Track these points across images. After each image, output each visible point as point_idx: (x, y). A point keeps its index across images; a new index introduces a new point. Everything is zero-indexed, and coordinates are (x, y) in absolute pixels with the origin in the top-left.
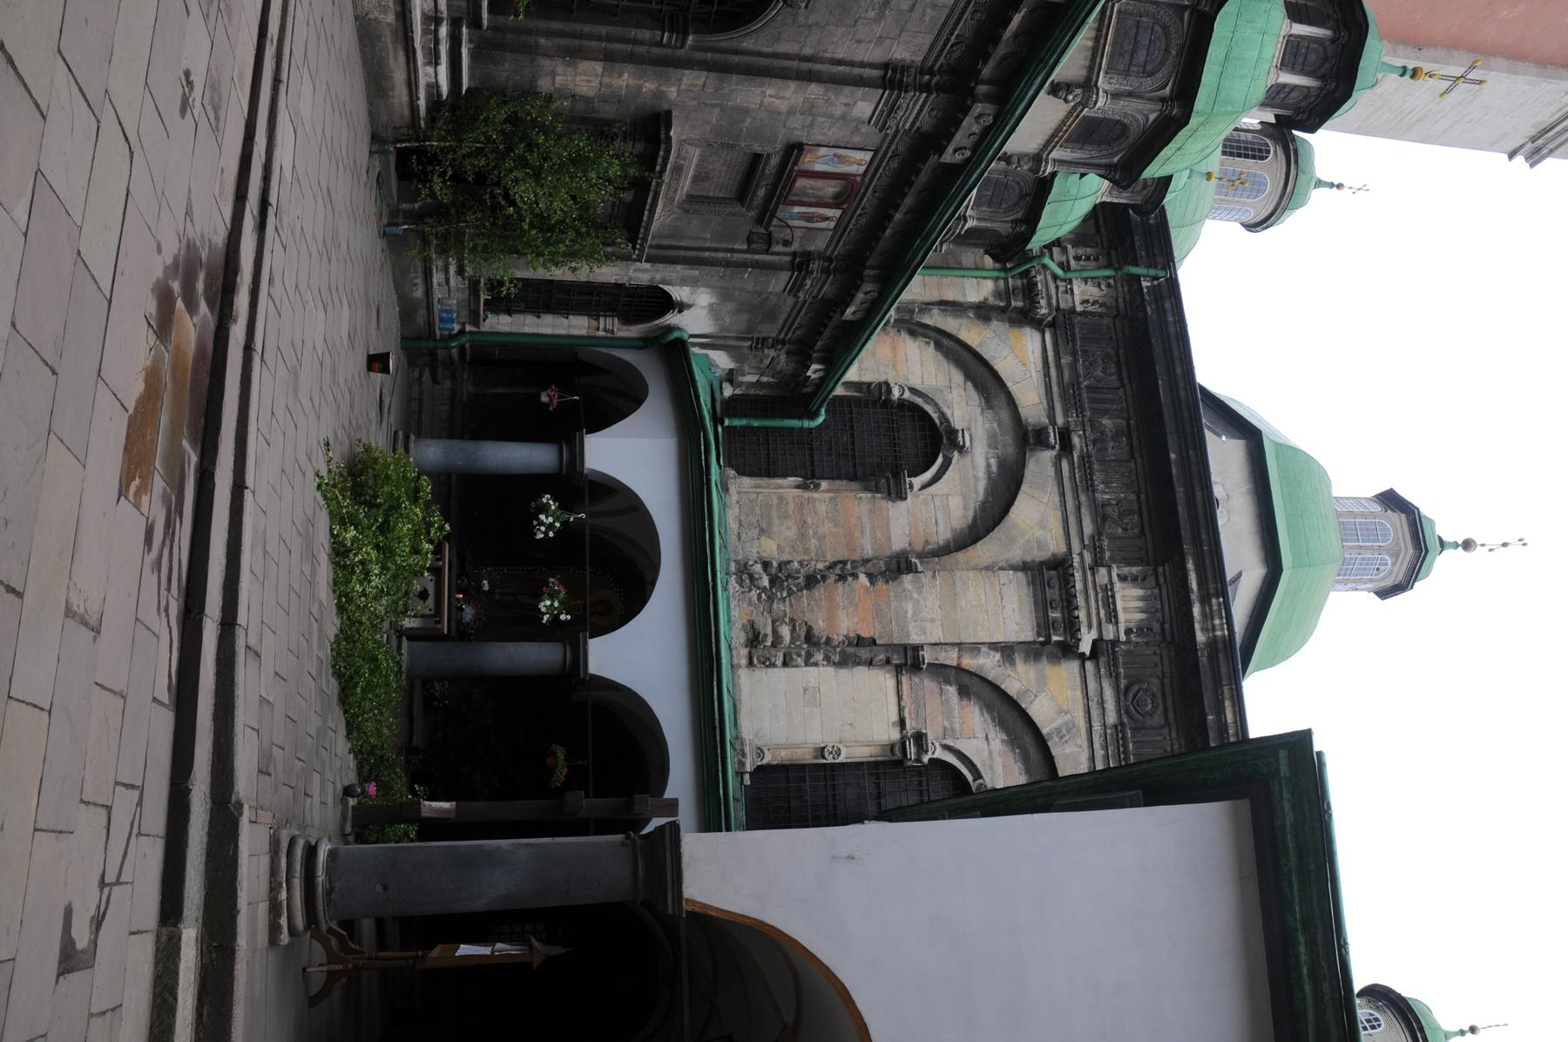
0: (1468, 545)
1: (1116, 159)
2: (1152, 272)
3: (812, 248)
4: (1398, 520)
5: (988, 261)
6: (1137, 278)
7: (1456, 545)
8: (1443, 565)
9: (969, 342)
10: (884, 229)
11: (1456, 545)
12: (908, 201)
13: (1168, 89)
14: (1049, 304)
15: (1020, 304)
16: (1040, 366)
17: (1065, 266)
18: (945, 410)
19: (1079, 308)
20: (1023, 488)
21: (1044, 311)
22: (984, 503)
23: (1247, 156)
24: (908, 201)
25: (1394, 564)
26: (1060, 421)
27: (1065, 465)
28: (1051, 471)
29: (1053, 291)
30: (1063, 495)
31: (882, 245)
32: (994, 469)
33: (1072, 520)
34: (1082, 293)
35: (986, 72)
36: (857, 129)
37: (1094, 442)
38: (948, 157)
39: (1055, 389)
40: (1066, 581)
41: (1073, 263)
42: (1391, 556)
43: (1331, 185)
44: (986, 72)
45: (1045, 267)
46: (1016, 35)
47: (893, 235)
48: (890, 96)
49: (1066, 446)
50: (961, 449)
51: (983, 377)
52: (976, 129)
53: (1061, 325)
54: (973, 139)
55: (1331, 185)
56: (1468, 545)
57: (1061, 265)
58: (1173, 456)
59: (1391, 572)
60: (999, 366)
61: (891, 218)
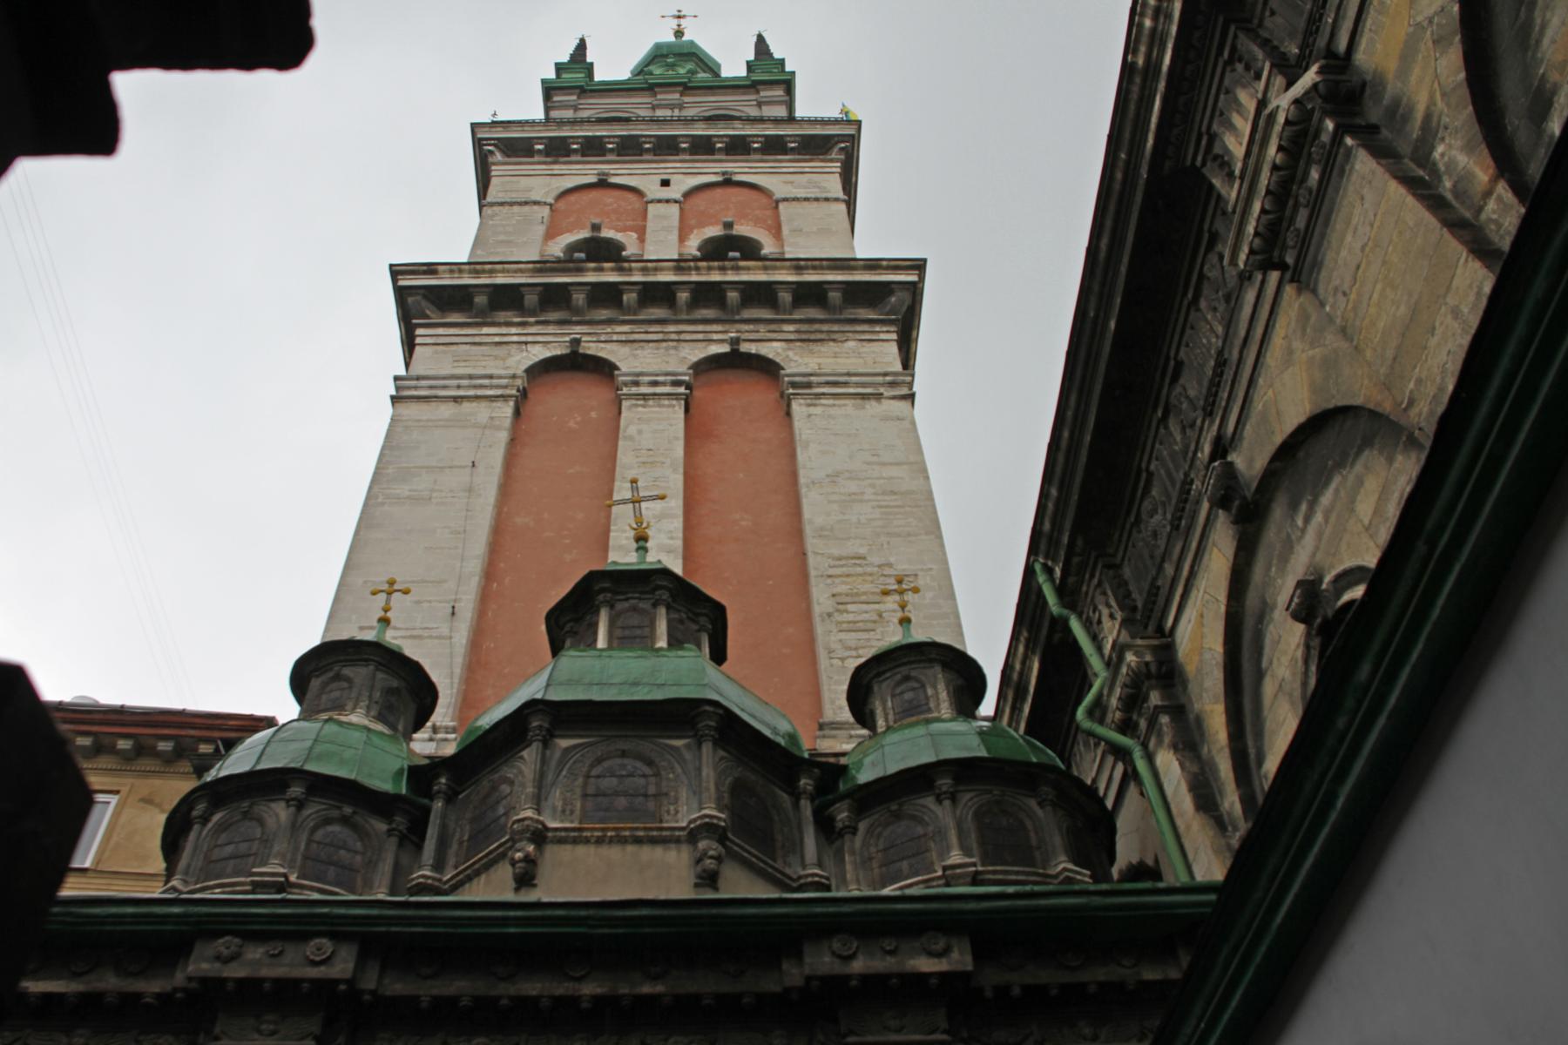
6: (1060, 591)
10: (652, 999)
18: (1300, 663)
22: (1340, 465)
24: (532, 987)
28: (1248, 430)
30: (1252, 382)
31: (705, 984)
33: (1259, 331)
35: (152, 986)
37: (1192, 425)
38: (343, 965)
39: (1194, 545)
40: (1272, 233)
44: (152, 986)
46: (76, 975)
47: (655, 978)
52: (255, 953)
58: (1112, 324)
61: (596, 999)
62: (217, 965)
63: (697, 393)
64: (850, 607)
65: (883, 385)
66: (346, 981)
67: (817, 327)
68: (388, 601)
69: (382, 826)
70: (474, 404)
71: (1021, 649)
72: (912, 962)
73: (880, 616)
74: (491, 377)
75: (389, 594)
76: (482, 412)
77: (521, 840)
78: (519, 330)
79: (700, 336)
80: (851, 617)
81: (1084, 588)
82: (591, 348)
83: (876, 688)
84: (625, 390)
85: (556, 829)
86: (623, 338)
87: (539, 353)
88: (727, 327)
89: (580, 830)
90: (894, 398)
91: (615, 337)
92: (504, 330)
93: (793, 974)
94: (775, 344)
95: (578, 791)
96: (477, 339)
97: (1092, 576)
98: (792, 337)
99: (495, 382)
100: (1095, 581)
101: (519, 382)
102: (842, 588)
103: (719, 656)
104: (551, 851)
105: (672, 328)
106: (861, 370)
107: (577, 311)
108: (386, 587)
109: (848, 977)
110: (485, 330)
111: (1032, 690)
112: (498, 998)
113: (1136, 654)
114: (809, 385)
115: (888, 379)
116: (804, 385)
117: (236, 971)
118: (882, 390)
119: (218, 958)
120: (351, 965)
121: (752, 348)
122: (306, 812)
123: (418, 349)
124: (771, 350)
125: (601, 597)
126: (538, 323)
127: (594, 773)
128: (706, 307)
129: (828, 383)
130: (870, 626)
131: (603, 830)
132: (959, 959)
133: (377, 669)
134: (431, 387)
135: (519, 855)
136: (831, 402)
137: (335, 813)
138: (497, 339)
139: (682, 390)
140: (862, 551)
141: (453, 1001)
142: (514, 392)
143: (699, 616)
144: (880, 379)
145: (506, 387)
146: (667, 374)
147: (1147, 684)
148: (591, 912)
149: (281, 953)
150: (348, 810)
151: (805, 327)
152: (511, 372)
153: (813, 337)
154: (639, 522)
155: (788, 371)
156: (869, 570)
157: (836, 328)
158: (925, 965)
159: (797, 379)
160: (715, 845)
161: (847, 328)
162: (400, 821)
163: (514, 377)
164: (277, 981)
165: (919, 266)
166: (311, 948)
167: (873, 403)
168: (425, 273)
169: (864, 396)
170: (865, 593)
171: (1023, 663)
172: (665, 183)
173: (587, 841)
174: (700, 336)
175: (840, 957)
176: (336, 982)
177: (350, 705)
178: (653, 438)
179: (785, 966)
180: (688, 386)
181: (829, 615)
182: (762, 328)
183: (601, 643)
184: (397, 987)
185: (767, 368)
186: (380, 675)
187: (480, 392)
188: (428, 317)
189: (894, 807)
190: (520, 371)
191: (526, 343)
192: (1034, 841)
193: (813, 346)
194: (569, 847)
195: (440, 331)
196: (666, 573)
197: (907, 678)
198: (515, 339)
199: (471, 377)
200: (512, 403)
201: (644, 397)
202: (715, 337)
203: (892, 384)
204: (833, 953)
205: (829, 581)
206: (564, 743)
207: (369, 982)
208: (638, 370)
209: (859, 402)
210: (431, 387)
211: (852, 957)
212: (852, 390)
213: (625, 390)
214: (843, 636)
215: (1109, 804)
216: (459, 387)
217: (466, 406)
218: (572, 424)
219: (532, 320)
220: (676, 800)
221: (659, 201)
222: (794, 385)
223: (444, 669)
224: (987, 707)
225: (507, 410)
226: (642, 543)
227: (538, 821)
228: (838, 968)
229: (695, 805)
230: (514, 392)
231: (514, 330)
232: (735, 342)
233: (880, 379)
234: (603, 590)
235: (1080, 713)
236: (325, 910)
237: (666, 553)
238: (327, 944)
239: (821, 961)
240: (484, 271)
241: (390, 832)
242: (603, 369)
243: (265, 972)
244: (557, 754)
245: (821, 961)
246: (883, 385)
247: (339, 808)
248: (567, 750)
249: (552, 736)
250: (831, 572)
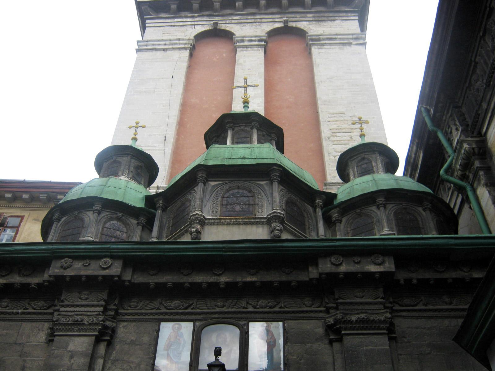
3: (320, 331)
12: (199, 278)
24: (199, 278)
36: (133, 343)
38: (116, 269)
44: (34, 280)
48: (61, 330)
52: (78, 265)
54: (87, 262)
61: (227, 283)
62: (62, 270)
63: (270, 45)
64: (338, 134)
65: (352, 39)
66: (118, 276)
67: (322, 14)
68: (136, 131)
69: (135, 222)
70: (172, 52)
71: (415, 148)
72: (367, 267)
73: (351, 138)
74: (179, 40)
75: (137, 128)
76: (176, 55)
77: (194, 223)
78: (191, 20)
79: (271, 20)
80: (338, 139)
81: (444, 118)
82: (223, 26)
83: (350, 163)
84: (238, 44)
85: (209, 219)
86: (237, 21)
87: (200, 29)
88: (282, 16)
89: (219, 219)
91: (233, 21)
92: (184, 20)
93: (313, 273)
94: (304, 23)
95: (219, 203)
96: (173, 24)
97: (448, 112)
98: (311, 19)
99: (181, 42)
100: (449, 114)
101: (191, 42)
102: (335, 126)
103: (280, 148)
104: (207, 228)
105: (258, 17)
106: (342, 33)
107: (216, 11)
108: (135, 125)
109: (338, 274)
110: (176, 20)
111: (419, 166)
112: (184, 283)
113: (468, 144)
114: (319, 40)
115: (354, 36)
116: (317, 40)
117: (69, 273)
118: (351, 41)
119: (62, 267)
120: (119, 270)
121: (294, 25)
122: (102, 215)
123: (147, 29)
124: (303, 25)
125: (228, 126)
126: (199, 16)
127: (226, 196)
128: (272, 7)
130: (347, 142)
131: (230, 219)
132: (389, 266)
133: (132, 158)
134: (153, 45)
135: (194, 230)
136: (329, 47)
137: (115, 216)
138: (181, 24)
139: (263, 43)
140: (343, 110)
141: (164, 284)
142: (189, 46)
143: (272, 132)
144: (351, 36)
145: (185, 44)
146: (256, 37)
147: (473, 157)
148: (224, 245)
149: (89, 264)
150: (120, 214)
152: (188, 37)
153: (320, 19)
154: (246, 96)
155: (310, 34)
156: (346, 118)
157: (331, 15)
158: (373, 268)
159: (314, 37)
160: (279, 225)
161: (336, 15)
162: (143, 220)
163: (189, 39)
164: (88, 277)
166: (101, 263)
167: (348, 47)
169: (343, 44)
170: (344, 128)
171: (416, 154)
173: (223, 224)
174: (271, 20)
175: (334, 264)
176: (112, 276)
177: (120, 173)
178: (250, 64)
179: (310, 269)
180: (266, 42)
181: (329, 138)
182: (298, 16)
184: (140, 279)
185: (300, 33)
186: (133, 161)
187: (174, 46)
188: (151, 15)
189: (358, 211)
190: (192, 36)
191: (194, 25)
192: (421, 226)
193: (320, 23)
194: (215, 227)
195: (157, 21)
196: (256, 114)
197: (364, 159)
198: (189, 23)
199: (170, 40)
200: (188, 51)
201: (246, 47)
202: (277, 20)
203: (356, 39)
204: (332, 263)
205: (329, 123)
206: (213, 183)
207: (128, 276)
208: (244, 35)
209: (342, 46)
210: (153, 45)
211: (340, 264)
212: (338, 42)
213: (238, 44)
214: (334, 146)
215: (456, 211)
216: (165, 44)
217: (169, 52)
218: (215, 60)
219: (196, 15)
220: (262, 206)
222: (312, 40)
223: (162, 157)
224: (400, 172)
225: (187, 53)
226: (246, 104)
227: (202, 215)
228: (334, 269)
229: (270, 208)
230: (189, 46)
231: (188, 20)
232: (286, 22)
233: (351, 36)
234: (229, 123)
235: (442, 172)
236: (108, 246)
237: (257, 106)
238: (109, 261)
239: (326, 266)
241: (138, 224)
242: (228, 36)
243: (83, 273)
244: (210, 188)
245: (326, 266)
246: (352, 39)
247: (116, 214)
248: (214, 186)
249: (207, 181)
250: (329, 119)
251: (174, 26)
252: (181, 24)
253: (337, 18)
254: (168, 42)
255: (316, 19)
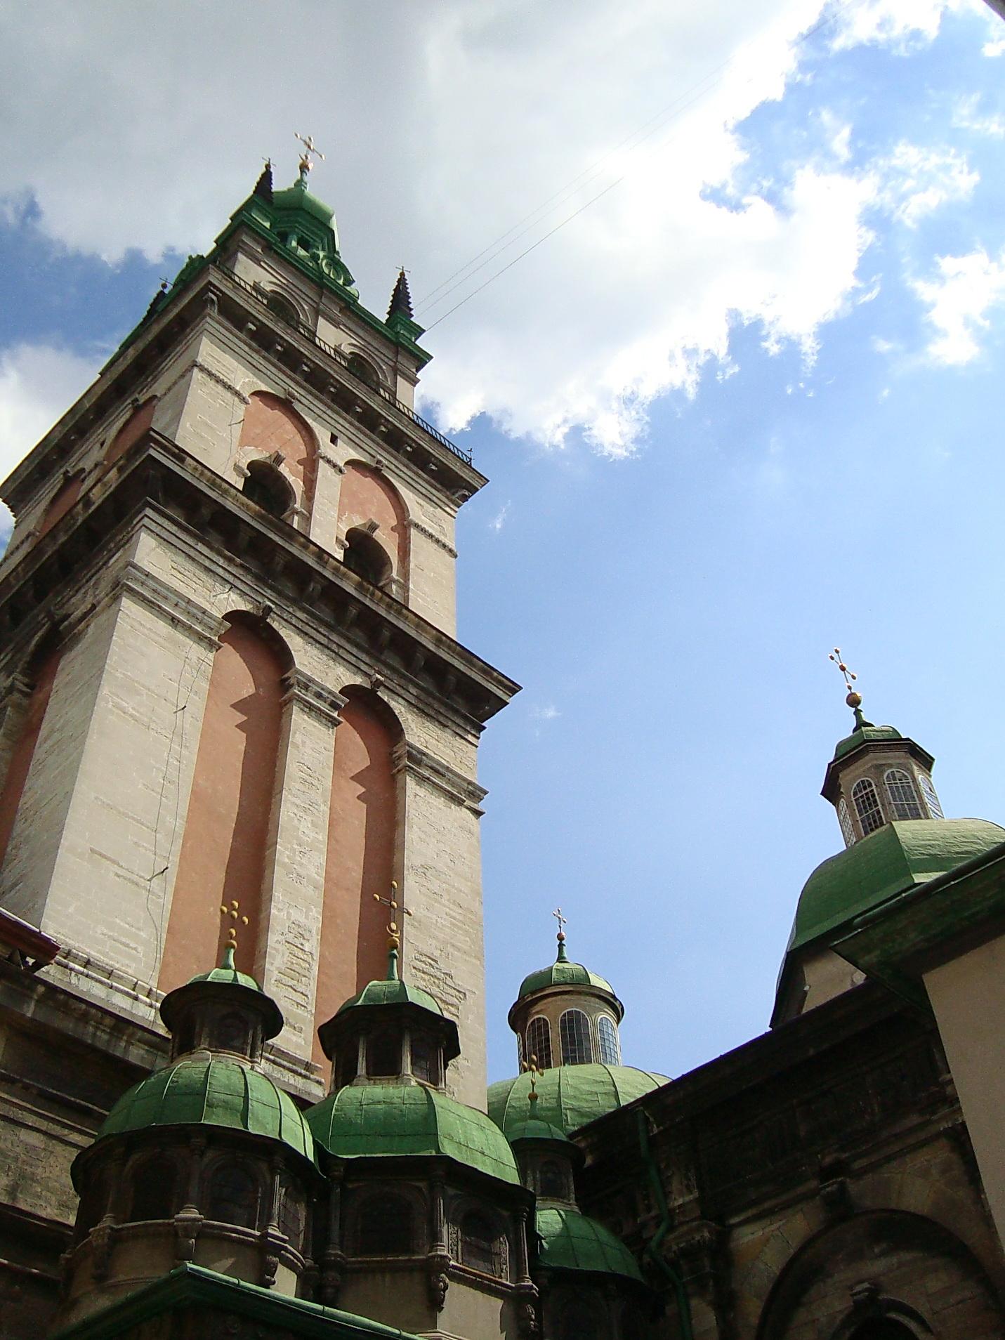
0: (853, 701)
1: (505, 1213)
2: (641, 1127)
4: (850, 780)
5: (670, 1309)
6: (652, 1141)
7: (857, 713)
8: (879, 718)
9: (759, 1311)
11: (857, 713)
13: (421, 1184)
14: (698, 1229)
15: (707, 1262)
16: (766, 1221)
17: (658, 1220)
18: (838, 1321)
19: (696, 1194)
20: (893, 1206)
21: (706, 1234)
23: (547, 1040)
25: (891, 766)
26: (813, 1184)
27: (857, 1165)
29: (685, 1228)
32: (884, 1245)
34: (681, 1195)
41: (653, 1213)
42: (882, 772)
43: (561, 946)
45: (661, 1244)
49: (838, 1169)
50: (875, 1290)
51: (797, 1279)
53: (719, 1210)
55: (561, 946)
56: (853, 701)
57: (658, 1226)
59: (900, 765)
60: (776, 1270)
79: (353, 660)
86: (300, 625)
90: (470, 809)
91: (294, 621)
92: (216, 558)
96: (192, 553)
110: (200, 547)
116: (417, 757)
126: (242, 566)
129: (432, 768)
138: (207, 563)
140: (437, 953)
151: (423, 696)
165: (513, 689)
168: (174, 455)
172: (334, 439)
174: (353, 660)
182: (395, 677)
183: (407, 1067)
195: (166, 523)
219: (238, 560)
221: (329, 461)
222: (410, 757)
232: (378, 684)
240: (220, 487)
251: (193, 559)
252: (207, 563)
253: (450, 724)
254: (182, 604)
255: (420, 705)
